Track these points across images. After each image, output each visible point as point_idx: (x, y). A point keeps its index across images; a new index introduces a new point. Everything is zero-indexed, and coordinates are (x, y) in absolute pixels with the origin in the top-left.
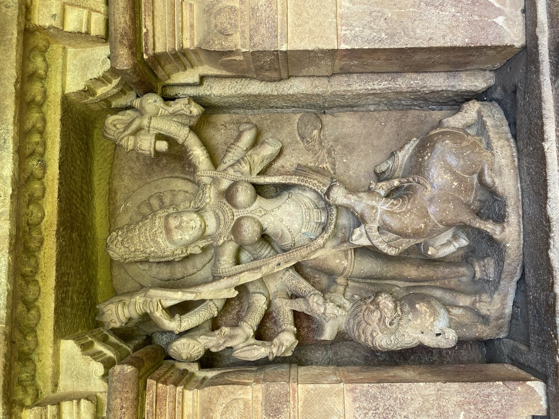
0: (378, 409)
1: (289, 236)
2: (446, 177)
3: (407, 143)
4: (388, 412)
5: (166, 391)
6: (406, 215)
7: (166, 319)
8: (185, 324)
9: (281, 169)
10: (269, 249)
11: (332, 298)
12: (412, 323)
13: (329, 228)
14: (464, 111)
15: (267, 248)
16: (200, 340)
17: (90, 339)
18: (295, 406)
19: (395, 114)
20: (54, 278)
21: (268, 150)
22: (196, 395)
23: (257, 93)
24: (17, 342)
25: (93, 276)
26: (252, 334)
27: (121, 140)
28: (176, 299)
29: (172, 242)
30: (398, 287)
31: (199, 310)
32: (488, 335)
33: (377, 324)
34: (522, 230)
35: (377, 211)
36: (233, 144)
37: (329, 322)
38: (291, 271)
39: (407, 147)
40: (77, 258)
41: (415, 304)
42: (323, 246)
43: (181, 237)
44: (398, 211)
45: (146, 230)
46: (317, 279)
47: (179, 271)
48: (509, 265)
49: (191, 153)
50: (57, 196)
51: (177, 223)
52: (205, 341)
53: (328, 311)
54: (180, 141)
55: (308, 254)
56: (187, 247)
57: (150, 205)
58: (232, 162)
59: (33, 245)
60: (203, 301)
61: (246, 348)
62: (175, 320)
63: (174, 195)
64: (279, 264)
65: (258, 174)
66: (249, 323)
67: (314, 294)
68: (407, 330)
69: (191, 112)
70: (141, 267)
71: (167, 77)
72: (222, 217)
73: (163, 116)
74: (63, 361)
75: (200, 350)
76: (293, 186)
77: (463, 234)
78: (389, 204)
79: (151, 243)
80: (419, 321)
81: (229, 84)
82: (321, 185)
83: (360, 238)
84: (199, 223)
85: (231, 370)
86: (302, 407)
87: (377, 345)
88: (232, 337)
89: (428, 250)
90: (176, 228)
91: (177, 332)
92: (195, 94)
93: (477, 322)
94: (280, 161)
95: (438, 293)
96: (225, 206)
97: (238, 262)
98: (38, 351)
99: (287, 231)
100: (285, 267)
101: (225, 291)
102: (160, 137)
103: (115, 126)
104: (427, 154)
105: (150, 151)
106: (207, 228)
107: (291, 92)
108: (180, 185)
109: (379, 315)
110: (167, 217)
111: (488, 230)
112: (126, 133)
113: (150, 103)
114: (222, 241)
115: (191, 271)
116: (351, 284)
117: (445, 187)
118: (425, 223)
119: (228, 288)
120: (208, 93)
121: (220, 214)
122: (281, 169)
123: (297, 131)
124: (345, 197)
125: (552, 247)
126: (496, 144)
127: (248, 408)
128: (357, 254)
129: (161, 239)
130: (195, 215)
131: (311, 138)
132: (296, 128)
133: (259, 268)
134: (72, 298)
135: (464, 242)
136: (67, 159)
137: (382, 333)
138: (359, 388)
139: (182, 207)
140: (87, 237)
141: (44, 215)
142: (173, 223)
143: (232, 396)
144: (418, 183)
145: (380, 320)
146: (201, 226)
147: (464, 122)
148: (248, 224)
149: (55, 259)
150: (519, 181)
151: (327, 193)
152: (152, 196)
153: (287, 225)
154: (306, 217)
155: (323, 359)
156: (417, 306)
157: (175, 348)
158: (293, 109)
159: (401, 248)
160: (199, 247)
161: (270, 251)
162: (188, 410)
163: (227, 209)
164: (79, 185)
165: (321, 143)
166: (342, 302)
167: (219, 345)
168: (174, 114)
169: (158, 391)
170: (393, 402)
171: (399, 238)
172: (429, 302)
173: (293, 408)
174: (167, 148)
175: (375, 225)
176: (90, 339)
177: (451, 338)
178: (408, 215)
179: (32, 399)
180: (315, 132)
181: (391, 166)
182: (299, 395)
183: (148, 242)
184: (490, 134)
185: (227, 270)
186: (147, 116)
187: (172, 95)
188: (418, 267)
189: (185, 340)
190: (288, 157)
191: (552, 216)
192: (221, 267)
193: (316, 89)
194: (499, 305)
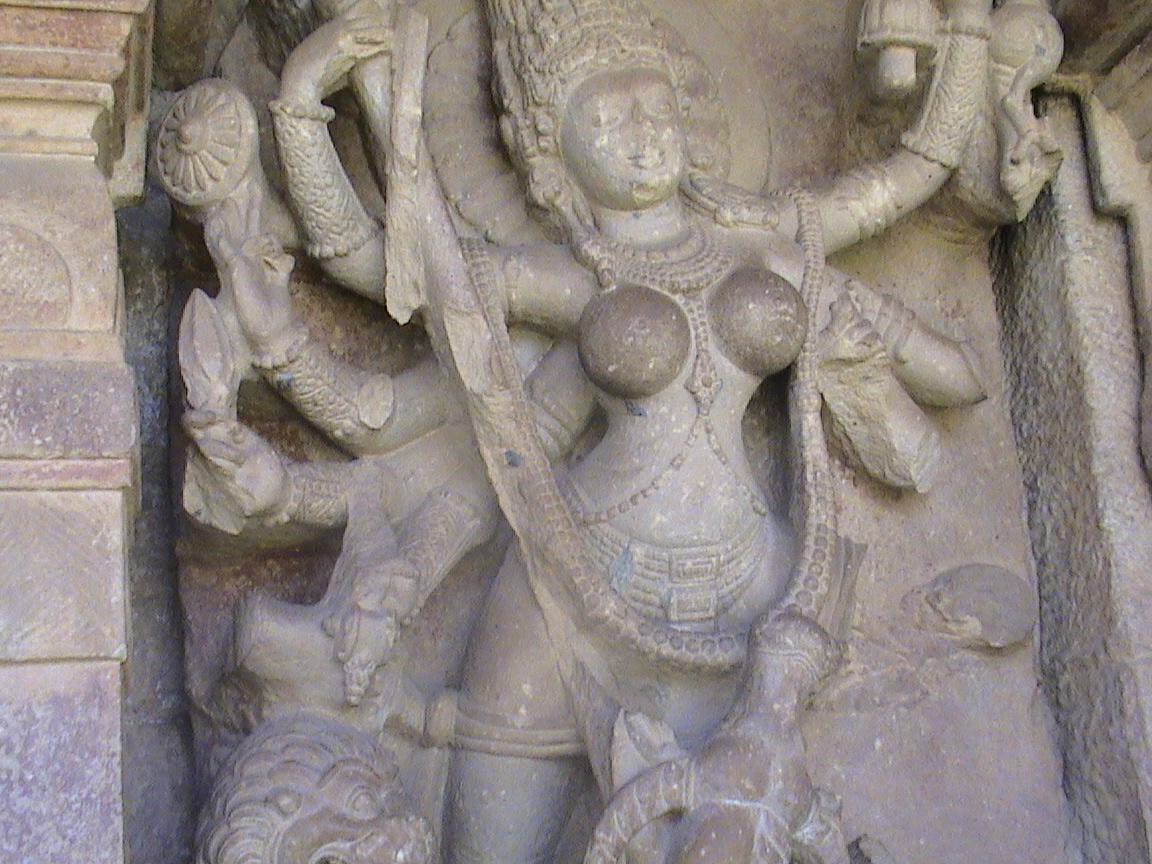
0: (26, 793)
4: (15, 830)
5: (102, 48)
8: (305, 133)
13: (662, 637)
15: (556, 437)
16: (245, 184)
18: (44, 476)
22: (78, 147)
26: (268, 363)
29: (583, 96)
33: (327, 810)
35: (747, 795)
37: (319, 638)
42: (589, 623)
43: (603, 119)
45: (618, 15)
49: (872, 171)
51: (647, 109)
52: (240, 202)
54: (909, 139)
55: (559, 565)
62: (317, 103)
64: (513, 461)
72: (674, 255)
73: (992, 77)
75: (210, 184)
78: (775, 846)
79: (576, 32)
81: (1111, 308)
83: (638, 747)
84: (653, 179)
86: (42, 503)
88: (264, 291)
90: (636, 104)
91: (276, 106)
92: (1061, 200)
96: (716, 264)
99: (634, 486)
100: (499, 488)
102: (925, 59)
106: (628, 214)
109: (358, 816)
113: (1033, 32)
116: (436, 758)
120: (1069, 240)
121: (688, 250)
124: (790, 679)
127: (37, 316)
131: (951, 609)
132: (978, 559)
138: (106, 718)
143: (75, 265)
145: (340, 819)
146: (642, 186)
148: (666, 335)
151: (791, 615)
153: (660, 483)
154: (689, 556)
157: (221, 100)
162: (22, 118)
163: (708, 270)
166: (379, 700)
169: (108, 20)
170: (52, 849)
173: (37, 470)
174: (896, 83)
180: (973, 626)
182: (83, 495)
183: (577, 22)
186: (988, 25)
190: (874, 527)
193: (1130, 609)
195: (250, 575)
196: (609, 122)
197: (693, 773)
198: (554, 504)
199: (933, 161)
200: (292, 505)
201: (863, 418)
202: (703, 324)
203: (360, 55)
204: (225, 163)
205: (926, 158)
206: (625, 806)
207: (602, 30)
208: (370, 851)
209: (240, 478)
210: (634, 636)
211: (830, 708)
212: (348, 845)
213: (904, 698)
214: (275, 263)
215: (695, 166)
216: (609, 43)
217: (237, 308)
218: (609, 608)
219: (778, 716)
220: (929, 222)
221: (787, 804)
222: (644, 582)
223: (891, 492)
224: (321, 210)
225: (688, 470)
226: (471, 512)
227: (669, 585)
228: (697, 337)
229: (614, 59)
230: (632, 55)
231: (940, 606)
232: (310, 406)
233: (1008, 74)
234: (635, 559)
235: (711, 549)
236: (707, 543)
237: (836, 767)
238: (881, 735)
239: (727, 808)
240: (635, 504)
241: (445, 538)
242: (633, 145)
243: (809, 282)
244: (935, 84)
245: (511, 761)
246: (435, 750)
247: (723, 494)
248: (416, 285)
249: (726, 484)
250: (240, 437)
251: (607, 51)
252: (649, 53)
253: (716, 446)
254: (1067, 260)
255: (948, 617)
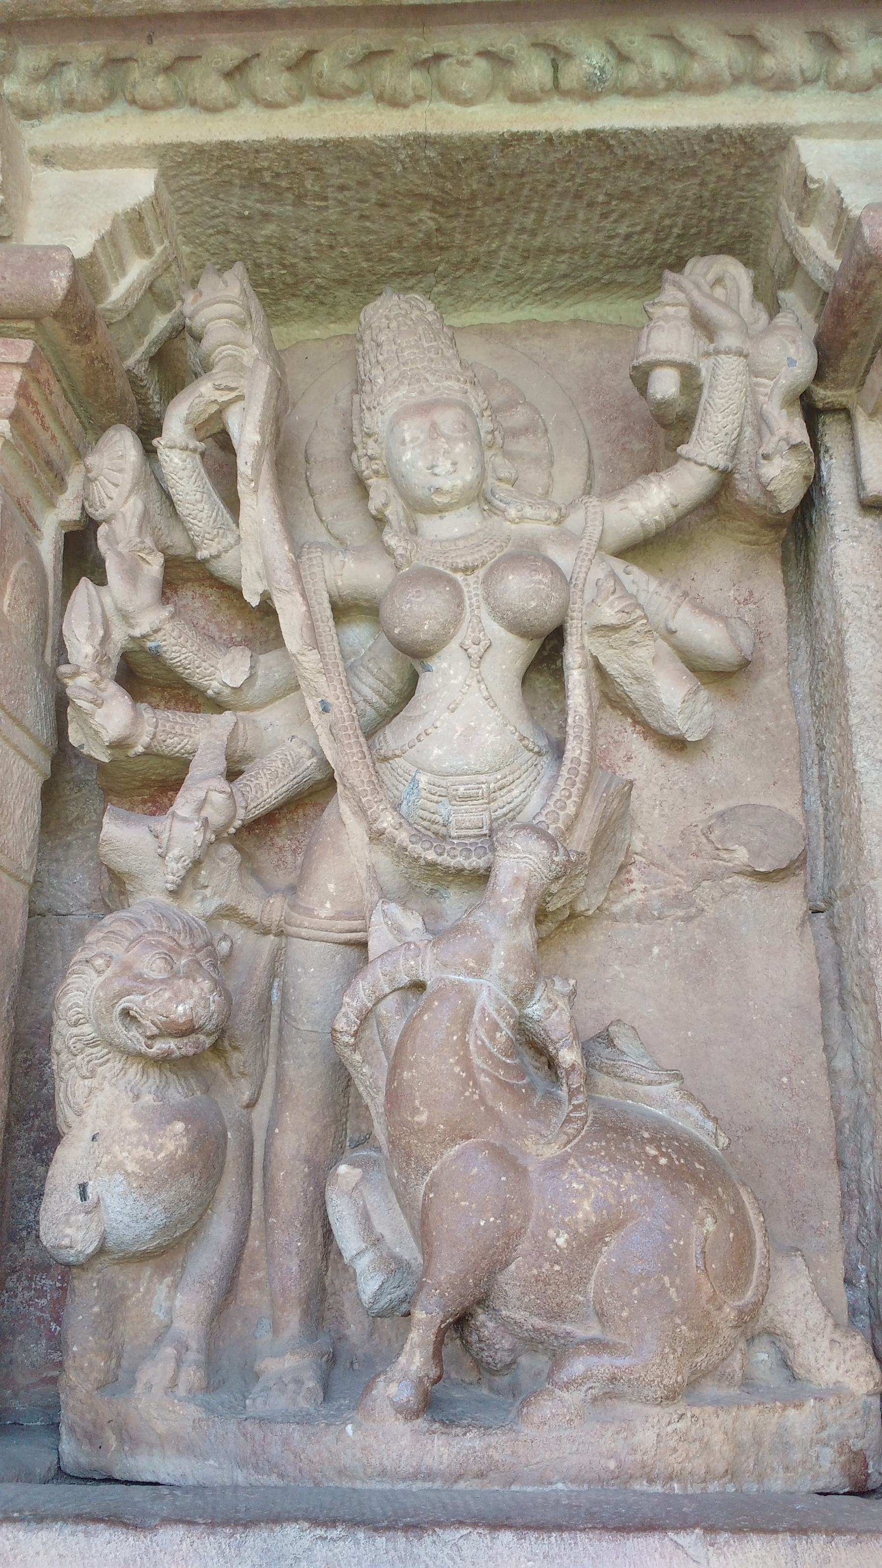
1: (409, 735)
2: (586, 1206)
3: (705, 1109)
6: (457, 1063)
7: (191, 407)
8: (176, 460)
9: (621, 754)
10: (375, 698)
11: (223, 865)
12: (128, 1101)
13: (427, 845)
14: (837, 1336)
15: (381, 696)
16: (131, 500)
17: (158, 249)
19: (820, 1122)
20: (307, 136)
21: (672, 695)
23: (850, 665)
24: (150, 49)
25: (333, 306)
26: (137, 633)
27: (675, 283)
28: (242, 427)
30: (251, 1105)
31: (214, 503)
32: (73, 1389)
34: (401, 1486)
35: (470, 972)
36: (685, 594)
37: (149, 838)
38: (310, 762)
39: (694, 1111)
40: (369, 232)
41: (185, 1119)
42: (377, 836)
43: (408, 438)
44: (470, 1039)
46: (290, 858)
47: (328, 480)
48: (286, 1442)
50: (514, 130)
52: (129, 515)
53: (178, 826)
54: (683, 449)
55: (353, 788)
56: (386, 476)
57: (510, 405)
58: (632, 589)
59: (387, 75)
60: (233, 504)
61: (98, 610)
63: (537, 461)
64: (325, 708)
65: (595, 659)
66: (168, 627)
67: (231, 795)
68: (106, 1085)
69: (766, 457)
70: (348, 389)
71: (871, 406)
73: (752, 392)
74: (105, 175)
75: (108, 503)
76: (558, 750)
77: (400, 1293)
78: (494, 1015)
79: (395, 374)
80: (133, 1124)
82: (560, 824)
84: (446, 484)
85: (51, 600)
87: (69, 981)
88: (132, 574)
89: (353, 1164)
90: (434, 426)
92: (832, 498)
93: (118, 1365)
94: (645, 749)
95: (221, 1229)
97: (343, 609)
98: (133, 112)
100: (319, 731)
101: (258, 562)
102: (690, 379)
103: (719, 281)
104: (664, 1155)
105: (648, 351)
106: (436, 517)
107: (862, 764)
108: (569, 476)
110: (467, 408)
111: (402, 1360)
112: (695, 294)
114: (392, 541)
115: (327, 511)
117: (552, 1201)
118: (430, 1127)
119: (267, 573)
120: (837, 530)
122: (621, 754)
123: (742, 802)
124: (517, 879)
125: (319, 1532)
126: (716, 1422)
128: (353, 953)
129: (404, 394)
130: (469, 477)
131: (722, 840)
132: (753, 801)
133: (315, 644)
134: (266, 216)
135: (369, 1285)
136: (621, 166)
137: (102, 986)
139: (499, 460)
140: (431, 278)
141: (467, 102)
142: (447, 419)
144: (568, 1120)
146: (438, 490)
147: (797, 1332)
149: (353, 134)
150: (574, 1487)
152: (536, 411)
154: (462, 783)
155: (67, 894)
156: (179, 1126)
158: (821, 810)
159: (357, 1057)
160: (385, 505)
161: (371, 704)
164: (564, 238)
165: (708, 875)
166: (208, 892)
167: (113, 541)
168: (761, 422)
171: (387, 1058)
172: (189, 1167)
174: (659, 396)
175: (428, 974)
176: (158, 249)
177: (68, 1231)
178: (457, 1069)
179: (15, 94)
180: (741, 855)
181: (628, 1059)
183: (398, 367)
184: (753, 1412)
185: (316, 570)
187: (826, 439)
188: (308, 1161)
189: (133, 459)
190: (661, 773)
191: (428, 1539)
192: (326, 557)
194: (161, 1427)
195: (154, 802)
196: (412, 441)
197: (429, 951)
198: (352, 741)
199: (702, 465)
200: (146, 739)
201: (637, 679)
202: (477, 595)
203: (220, 400)
204: (116, 485)
205: (696, 463)
206: (369, 977)
207: (416, 371)
208: (157, 1003)
209: (99, 717)
210: (405, 844)
211: (614, 918)
212: (142, 997)
213: (681, 913)
214: (148, 558)
215: (500, 480)
216: (418, 381)
217: (110, 591)
218: (387, 821)
219: (505, 909)
220: (725, 527)
221: (507, 981)
222: (429, 805)
223: (675, 745)
224: (195, 522)
225: (468, 714)
226: (308, 753)
227: (450, 807)
228: (471, 605)
229: (422, 392)
230: (438, 389)
231: (712, 837)
232: (180, 670)
233: (766, 386)
234: (421, 786)
235: (482, 778)
236: (478, 773)
237: (616, 967)
238: (658, 943)
239: (452, 983)
240: (420, 741)
241: (280, 771)
242: (430, 457)
243: (580, 563)
244: (703, 400)
245: (317, 944)
246: (272, 937)
247: (490, 732)
248: (258, 574)
249: (493, 724)
250: (102, 686)
251: (416, 386)
252: (452, 387)
253: (485, 694)
254: (835, 548)
255: (719, 846)
